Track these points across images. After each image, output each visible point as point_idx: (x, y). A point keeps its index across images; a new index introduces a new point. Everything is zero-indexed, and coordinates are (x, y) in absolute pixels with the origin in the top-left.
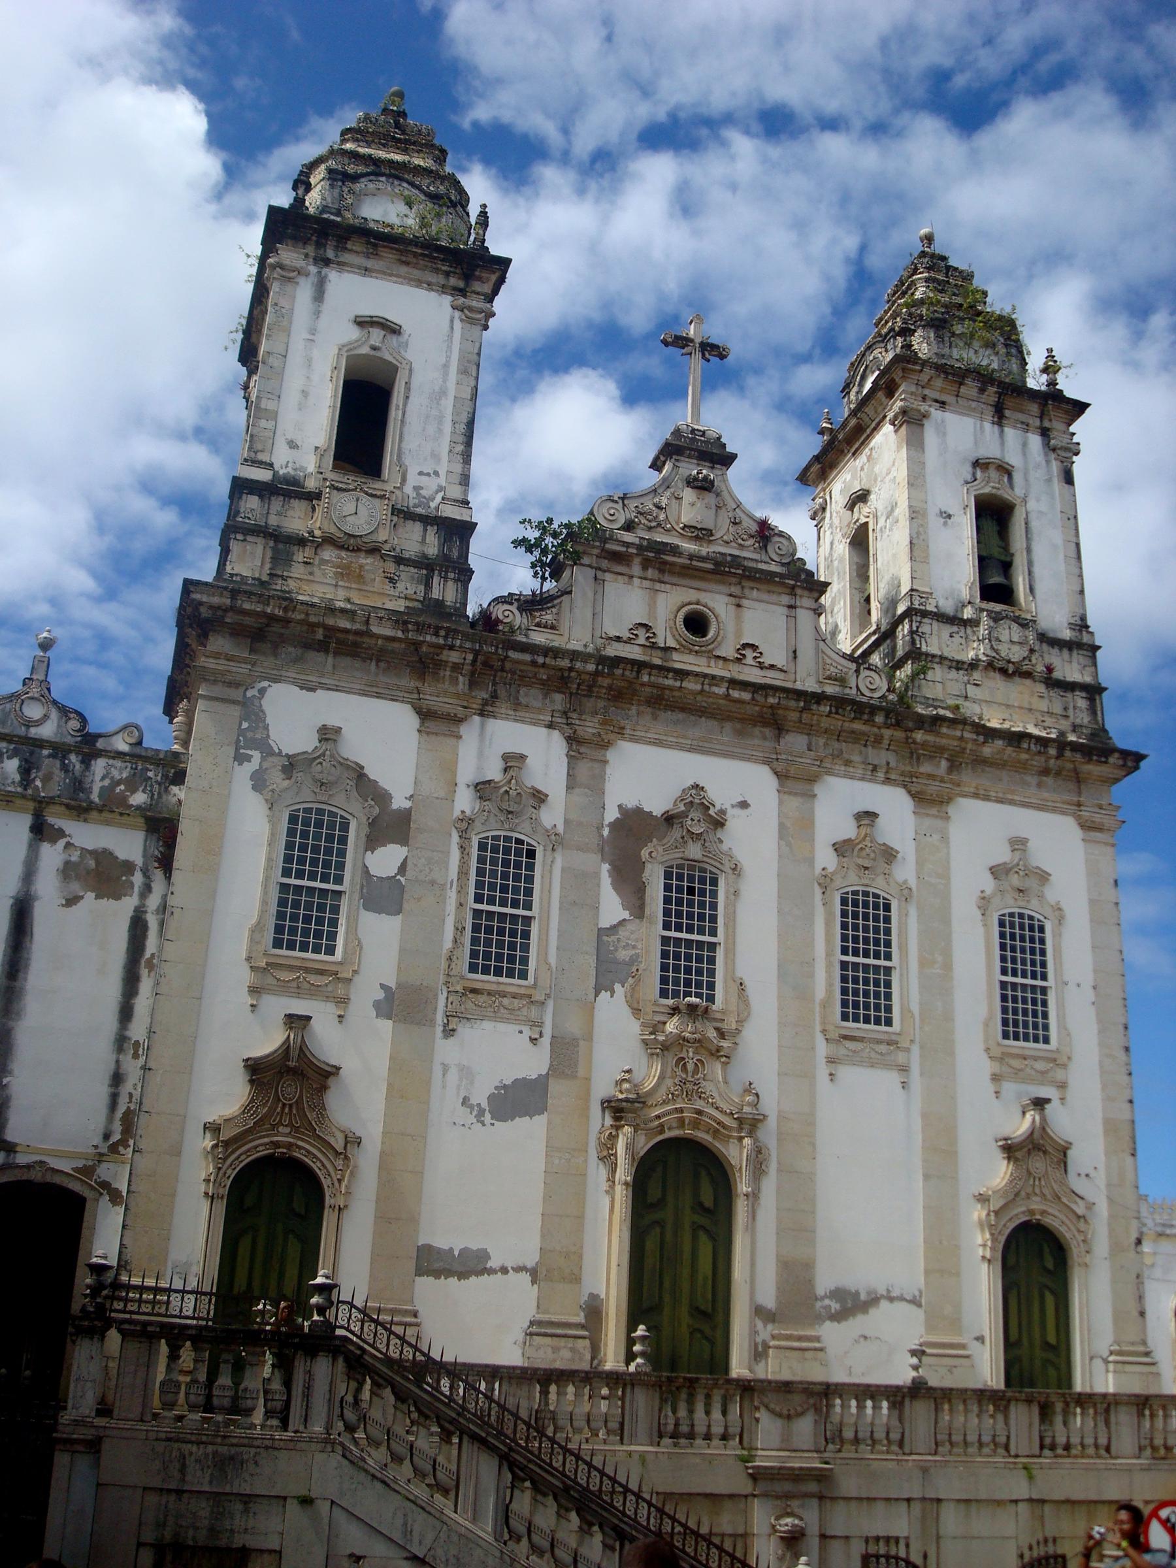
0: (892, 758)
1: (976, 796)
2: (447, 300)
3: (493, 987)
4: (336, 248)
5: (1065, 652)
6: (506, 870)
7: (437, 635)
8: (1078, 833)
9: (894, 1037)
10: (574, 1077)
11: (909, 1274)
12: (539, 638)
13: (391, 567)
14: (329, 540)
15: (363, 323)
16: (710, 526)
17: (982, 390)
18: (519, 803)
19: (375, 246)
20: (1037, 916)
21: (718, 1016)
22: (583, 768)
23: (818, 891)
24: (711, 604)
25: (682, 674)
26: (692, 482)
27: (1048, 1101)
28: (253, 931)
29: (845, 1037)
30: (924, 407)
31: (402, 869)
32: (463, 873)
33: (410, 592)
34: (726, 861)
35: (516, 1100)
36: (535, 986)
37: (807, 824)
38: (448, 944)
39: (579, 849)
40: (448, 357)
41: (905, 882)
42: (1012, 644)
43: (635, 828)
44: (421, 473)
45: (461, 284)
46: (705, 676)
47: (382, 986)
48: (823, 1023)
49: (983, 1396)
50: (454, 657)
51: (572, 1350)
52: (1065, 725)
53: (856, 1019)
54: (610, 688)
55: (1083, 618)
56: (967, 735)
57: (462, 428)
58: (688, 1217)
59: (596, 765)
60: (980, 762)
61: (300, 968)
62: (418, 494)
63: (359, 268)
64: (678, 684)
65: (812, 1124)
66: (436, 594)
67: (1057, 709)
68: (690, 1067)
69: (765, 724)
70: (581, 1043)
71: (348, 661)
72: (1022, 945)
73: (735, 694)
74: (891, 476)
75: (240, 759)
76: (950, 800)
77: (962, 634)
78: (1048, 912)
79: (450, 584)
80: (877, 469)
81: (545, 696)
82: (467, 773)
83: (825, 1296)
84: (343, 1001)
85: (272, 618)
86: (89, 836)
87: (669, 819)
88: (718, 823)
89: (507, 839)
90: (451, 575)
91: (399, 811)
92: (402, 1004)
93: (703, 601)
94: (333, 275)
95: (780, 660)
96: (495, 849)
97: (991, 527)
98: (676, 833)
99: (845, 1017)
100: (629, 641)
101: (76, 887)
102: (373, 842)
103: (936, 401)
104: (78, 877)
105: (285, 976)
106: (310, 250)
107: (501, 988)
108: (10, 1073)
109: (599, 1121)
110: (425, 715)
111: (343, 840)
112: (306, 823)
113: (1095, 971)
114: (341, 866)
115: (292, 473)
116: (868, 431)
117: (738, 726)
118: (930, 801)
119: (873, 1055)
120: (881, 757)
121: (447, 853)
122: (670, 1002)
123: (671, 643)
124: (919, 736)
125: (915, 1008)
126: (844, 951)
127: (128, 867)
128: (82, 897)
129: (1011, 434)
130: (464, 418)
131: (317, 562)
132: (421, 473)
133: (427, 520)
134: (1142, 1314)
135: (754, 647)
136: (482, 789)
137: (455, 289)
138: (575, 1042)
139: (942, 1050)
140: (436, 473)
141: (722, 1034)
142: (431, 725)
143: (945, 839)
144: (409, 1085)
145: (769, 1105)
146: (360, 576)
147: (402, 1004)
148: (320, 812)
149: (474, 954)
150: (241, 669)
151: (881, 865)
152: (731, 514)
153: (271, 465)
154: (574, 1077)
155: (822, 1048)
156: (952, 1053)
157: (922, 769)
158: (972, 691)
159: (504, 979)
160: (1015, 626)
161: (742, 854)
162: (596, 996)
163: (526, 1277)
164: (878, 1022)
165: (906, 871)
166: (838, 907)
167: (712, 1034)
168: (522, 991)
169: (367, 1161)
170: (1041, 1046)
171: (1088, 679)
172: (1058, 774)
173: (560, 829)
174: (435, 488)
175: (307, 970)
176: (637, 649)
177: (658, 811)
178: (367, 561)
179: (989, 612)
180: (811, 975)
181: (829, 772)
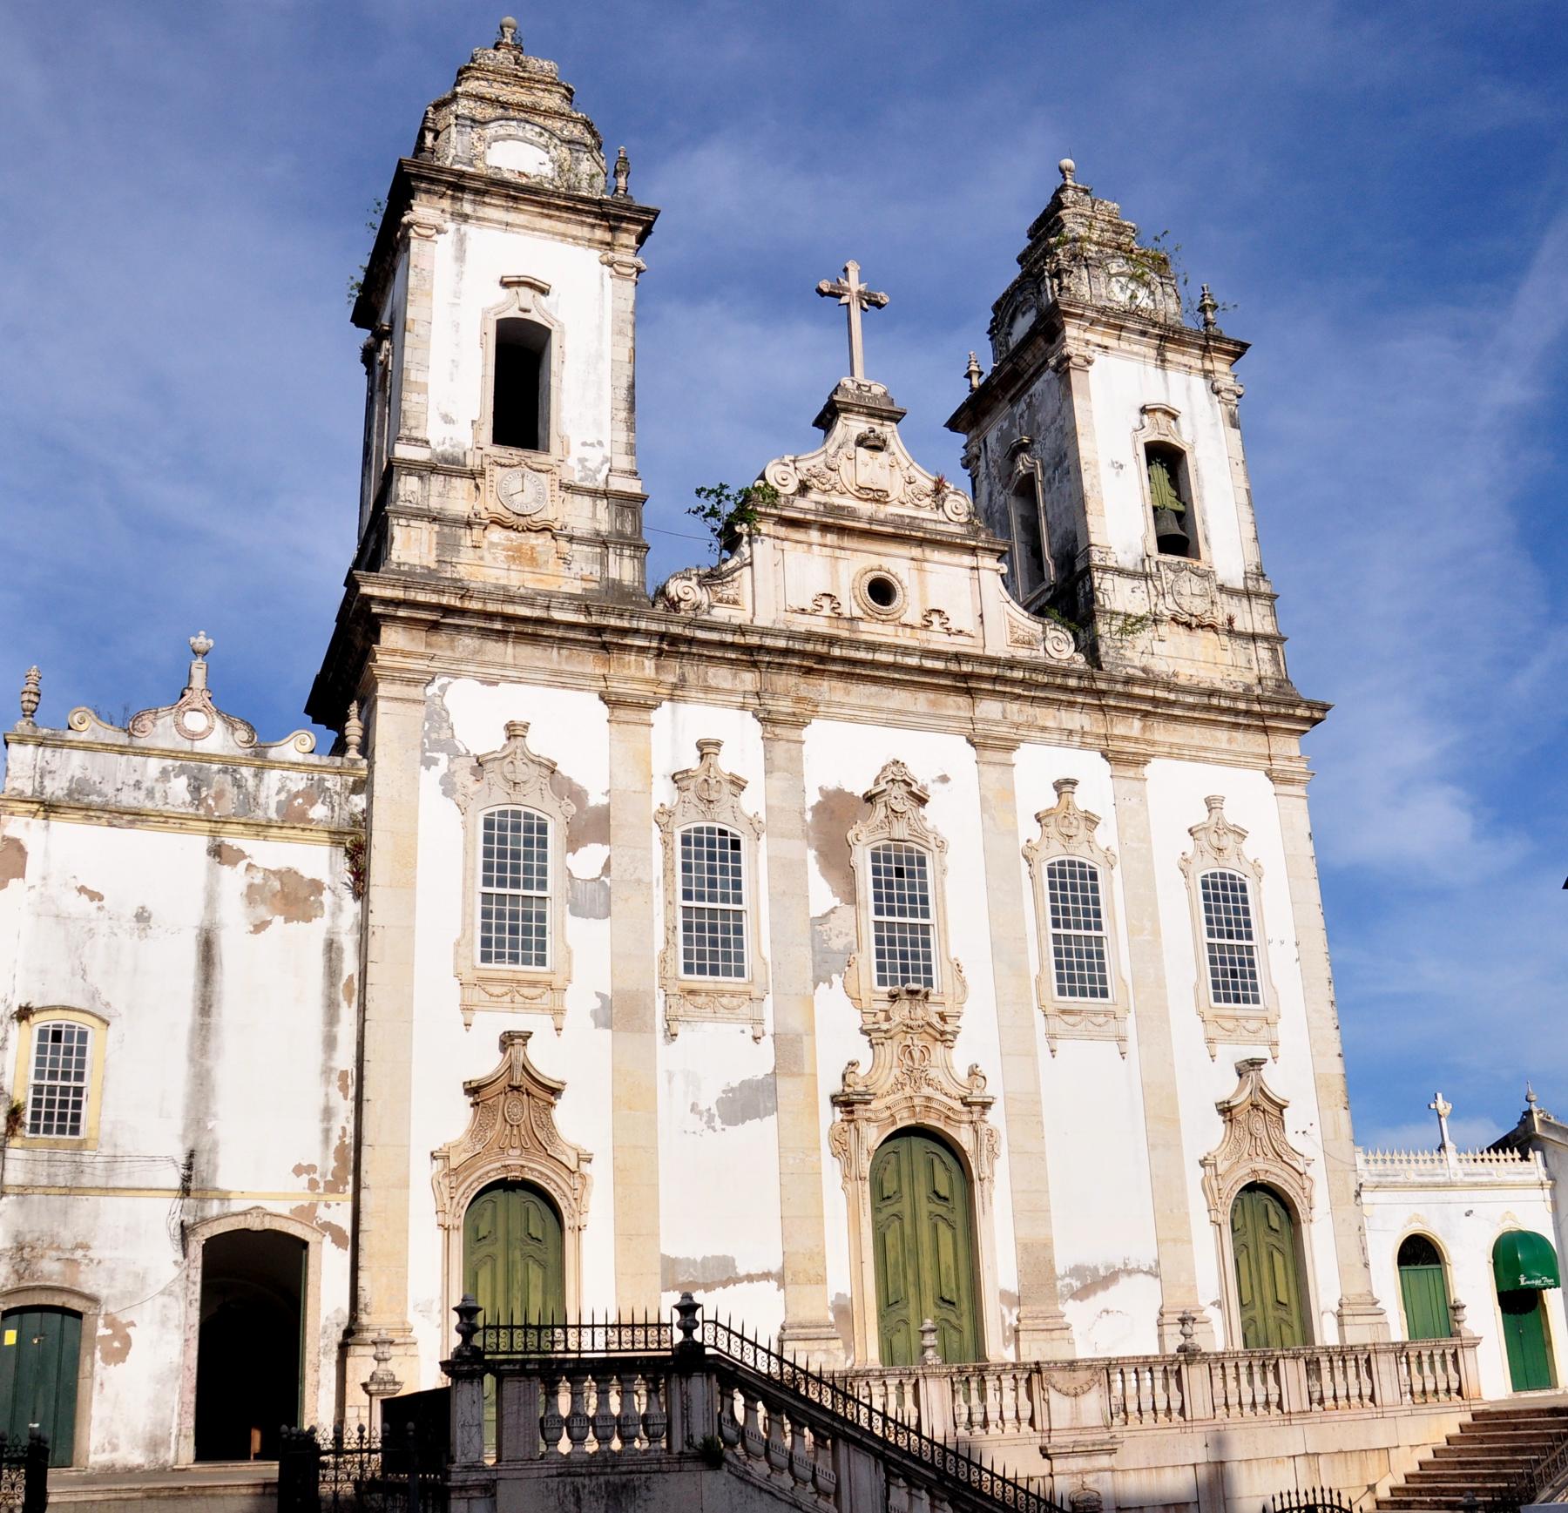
1: (1170, 755)
2: (595, 254)
3: (711, 986)
4: (474, 202)
5: (1245, 601)
7: (621, 616)
9: (1110, 1008)
10: (801, 1075)
12: (721, 614)
13: (563, 544)
18: (718, 792)
20: (1238, 875)
21: (937, 999)
22: (780, 748)
24: (893, 571)
25: (873, 647)
26: (861, 442)
27: (1263, 1062)
28: (458, 944)
29: (1064, 1012)
30: (1087, 352)
31: (607, 868)
32: (668, 871)
33: (586, 572)
34: (931, 839)
35: (745, 1103)
36: (751, 982)
37: (1008, 795)
38: (659, 945)
39: (782, 836)
40: (601, 317)
43: (837, 812)
44: (584, 444)
45: (608, 237)
46: (897, 646)
47: (598, 995)
48: (1039, 999)
49: (1148, 1363)
53: (1072, 993)
57: (623, 393)
58: (925, 1207)
59: (792, 746)
61: (512, 981)
62: (584, 467)
63: (500, 223)
64: (870, 656)
65: (1039, 1102)
66: (614, 573)
67: (1242, 662)
68: (917, 1054)
72: (1226, 903)
74: (1057, 425)
75: (429, 763)
77: (1144, 588)
78: (1248, 870)
80: (1039, 418)
81: (735, 676)
83: (1066, 1275)
84: (558, 1012)
86: (271, 854)
87: (870, 798)
88: (922, 801)
89: (711, 831)
90: (627, 552)
91: (597, 809)
92: (618, 1013)
93: (885, 567)
94: (469, 229)
95: (969, 625)
97: (1161, 473)
98: (880, 812)
101: (263, 912)
104: (263, 902)
105: (497, 990)
106: (446, 203)
107: (719, 987)
108: (215, 1116)
109: (830, 1116)
110: (612, 701)
111: (543, 843)
114: (543, 871)
115: (450, 450)
116: (1026, 376)
117: (932, 696)
119: (1091, 1027)
121: (649, 849)
122: (888, 988)
123: (857, 613)
126: (1056, 924)
127: (317, 886)
128: (270, 922)
129: (1173, 375)
131: (485, 544)
132: (584, 444)
133: (593, 493)
134: (1366, 1265)
137: (602, 243)
138: (798, 1038)
140: (600, 443)
141: (943, 1018)
142: (622, 714)
143: (1143, 801)
144: (633, 1098)
145: (993, 1089)
147: (618, 1013)
148: (516, 814)
151: (1082, 833)
152: (905, 473)
153: (427, 442)
156: (1168, 1021)
157: (1116, 732)
159: (720, 978)
161: (945, 833)
162: (815, 987)
163: (774, 1284)
164: (1094, 994)
165: (1105, 836)
167: (935, 1020)
168: (741, 988)
170: (1251, 1006)
173: (762, 816)
174: (600, 459)
175: (519, 981)
176: (824, 622)
177: (860, 793)
179: (1169, 566)
180: (1024, 951)
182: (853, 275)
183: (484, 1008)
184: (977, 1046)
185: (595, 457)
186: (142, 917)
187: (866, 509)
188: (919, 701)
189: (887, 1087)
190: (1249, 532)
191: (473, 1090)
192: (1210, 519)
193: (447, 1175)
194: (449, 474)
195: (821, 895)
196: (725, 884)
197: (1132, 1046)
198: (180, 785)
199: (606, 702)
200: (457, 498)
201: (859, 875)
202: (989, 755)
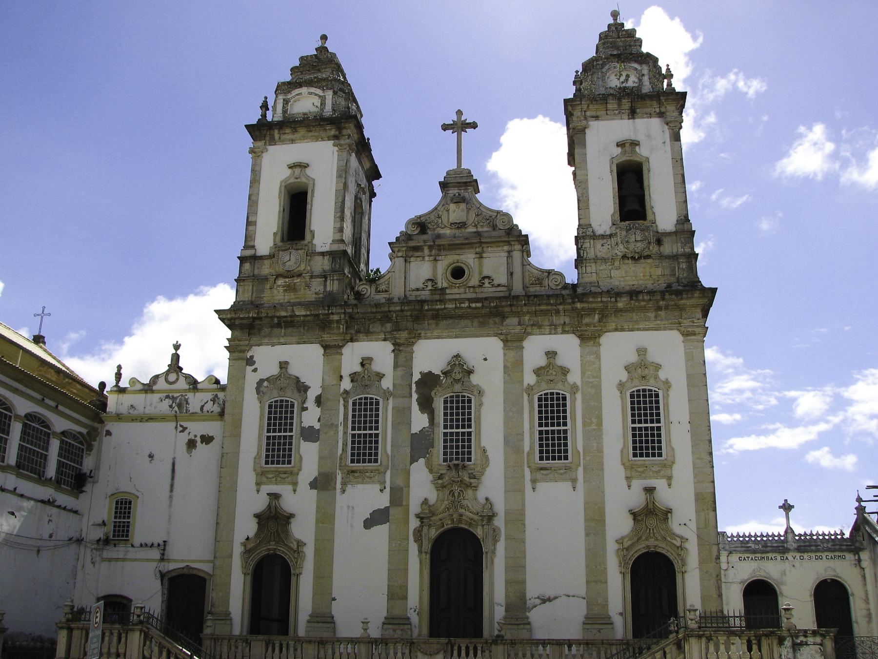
0: (567, 320)
1: (616, 330)
6: (365, 413)
8: (681, 338)
10: (401, 505)
11: (579, 585)
16: (464, 219)
19: (295, 128)
20: (653, 389)
22: (402, 358)
23: (526, 396)
29: (542, 469)
35: (376, 518)
38: (340, 452)
41: (575, 383)
43: (428, 381)
46: (455, 300)
51: (402, 630)
52: (673, 279)
54: (411, 316)
55: (686, 216)
56: (604, 299)
60: (618, 311)
66: (328, 289)
68: (456, 495)
69: (496, 316)
71: (290, 330)
73: (473, 305)
76: (600, 336)
78: (661, 385)
79: (335, 282)
82: (346, 371)
84: (295, 484)
85: (254, 318)
88: (470, 372)
96: (360, 404)
100: (423, 289)
103: (593, 117)
105: (270, 476)
110: (326, 347)
112: (276, 407)
113: (690, 413)
118: (589, 339)
119: (556, 475)
123: (445, 285)
125: (580, 448)
130: (340, 199)
135: (488, 277)
136: (354, 377)
139: (596, 468)
143: (598, 357)
144: (325, 519)
145: (500, 507)
146: (295, 289)
147: (322, 483)
149: (353, 455)
154: (401, 505)
155: (528, 475)
156: (602, 470)
158: (614, 273)
160: (638, 232)
164: (560, 458)
165: (575, 377)
169: (309, 551)
171: (688, 250)
172: (667, 308)
173: (391, 388)
175: (280, 473)
178: (297, 280)
181: (530, 334)
183: (265, 484)
184: (492, 486)
186: (151, 456)
191: (257, 516)
193: (245, 553)
196: (371, 422)
197: (580, 484)
199: (322, 346)
201: (436, 412)
202: (509, 344)
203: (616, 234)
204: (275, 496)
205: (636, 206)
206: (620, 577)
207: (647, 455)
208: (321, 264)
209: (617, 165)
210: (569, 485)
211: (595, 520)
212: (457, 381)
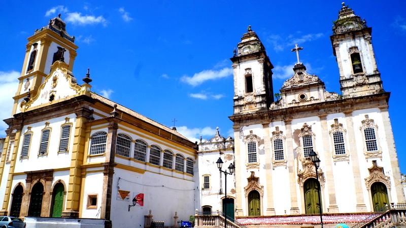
0: (340, 108)
1: (357, 109)
6: (278, 144)
14: (246, 104)
15: (246, 70)
17: (349, 34)
30: (338, 43)
32: (272, 146)
42: (360, 80)
50: (266, 115)
60: (357, 104)
70: (293, 167)
71: (252, 120)
72: (370, 135)
99: (336, 154)
102: (259, 145)
109: (297, 177)
110: (263, 125)
120: (337, 108)
124: (343, 103)
129: (357, 41)
144: (269, 178)
147: (266, 167)
150: (238, 126)
155: (333, 160)
165: (345, 127)
166: (333, 136)
181: (329, 114)
182: (296, 46)
185: (259, 90)
187: (300, 84)
188: (310, 113)
189: (305, 173)
190: (375, 63)
192: (365, 63)
194: (240, 99)
195: (295, 145)
197: (350, 162)
198: (216, 146)
200: (241, 102)
203: (353, 78)
204: (252, 172)
205: (359, 68)
206: (368, 192)
207: (372, 150)
208: (259, 99)
209: (351, 55)
210: (347, 162)
211: (357, 173)
212: (306, 131)
